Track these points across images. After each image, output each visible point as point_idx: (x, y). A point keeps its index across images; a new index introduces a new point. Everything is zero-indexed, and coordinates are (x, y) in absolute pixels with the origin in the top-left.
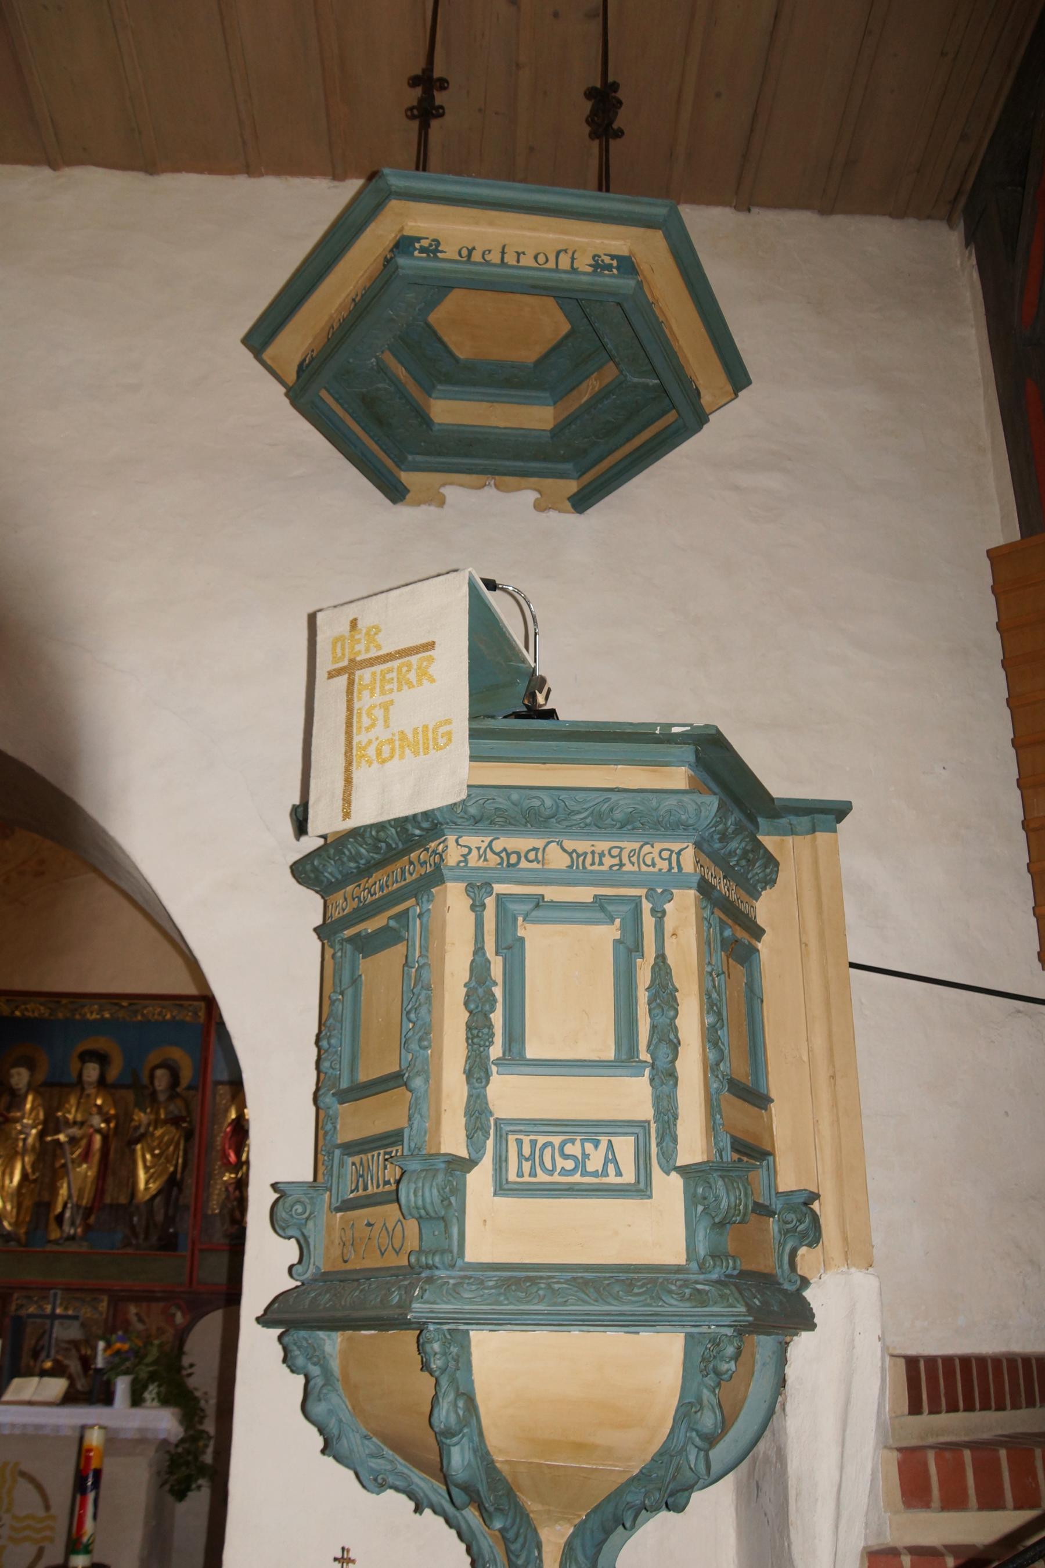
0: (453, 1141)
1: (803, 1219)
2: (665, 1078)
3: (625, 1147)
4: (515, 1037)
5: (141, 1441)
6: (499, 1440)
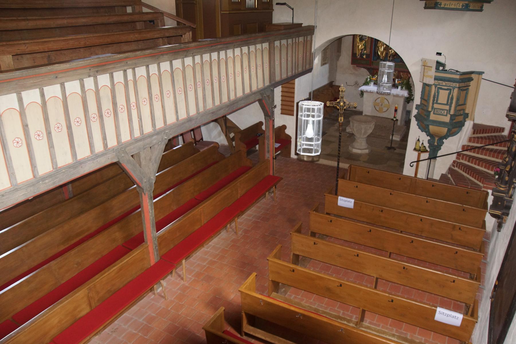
0: (430, 109)
2: (450, 107)
3: (446, 112)
4: (437, 100)
5: (402, 96)
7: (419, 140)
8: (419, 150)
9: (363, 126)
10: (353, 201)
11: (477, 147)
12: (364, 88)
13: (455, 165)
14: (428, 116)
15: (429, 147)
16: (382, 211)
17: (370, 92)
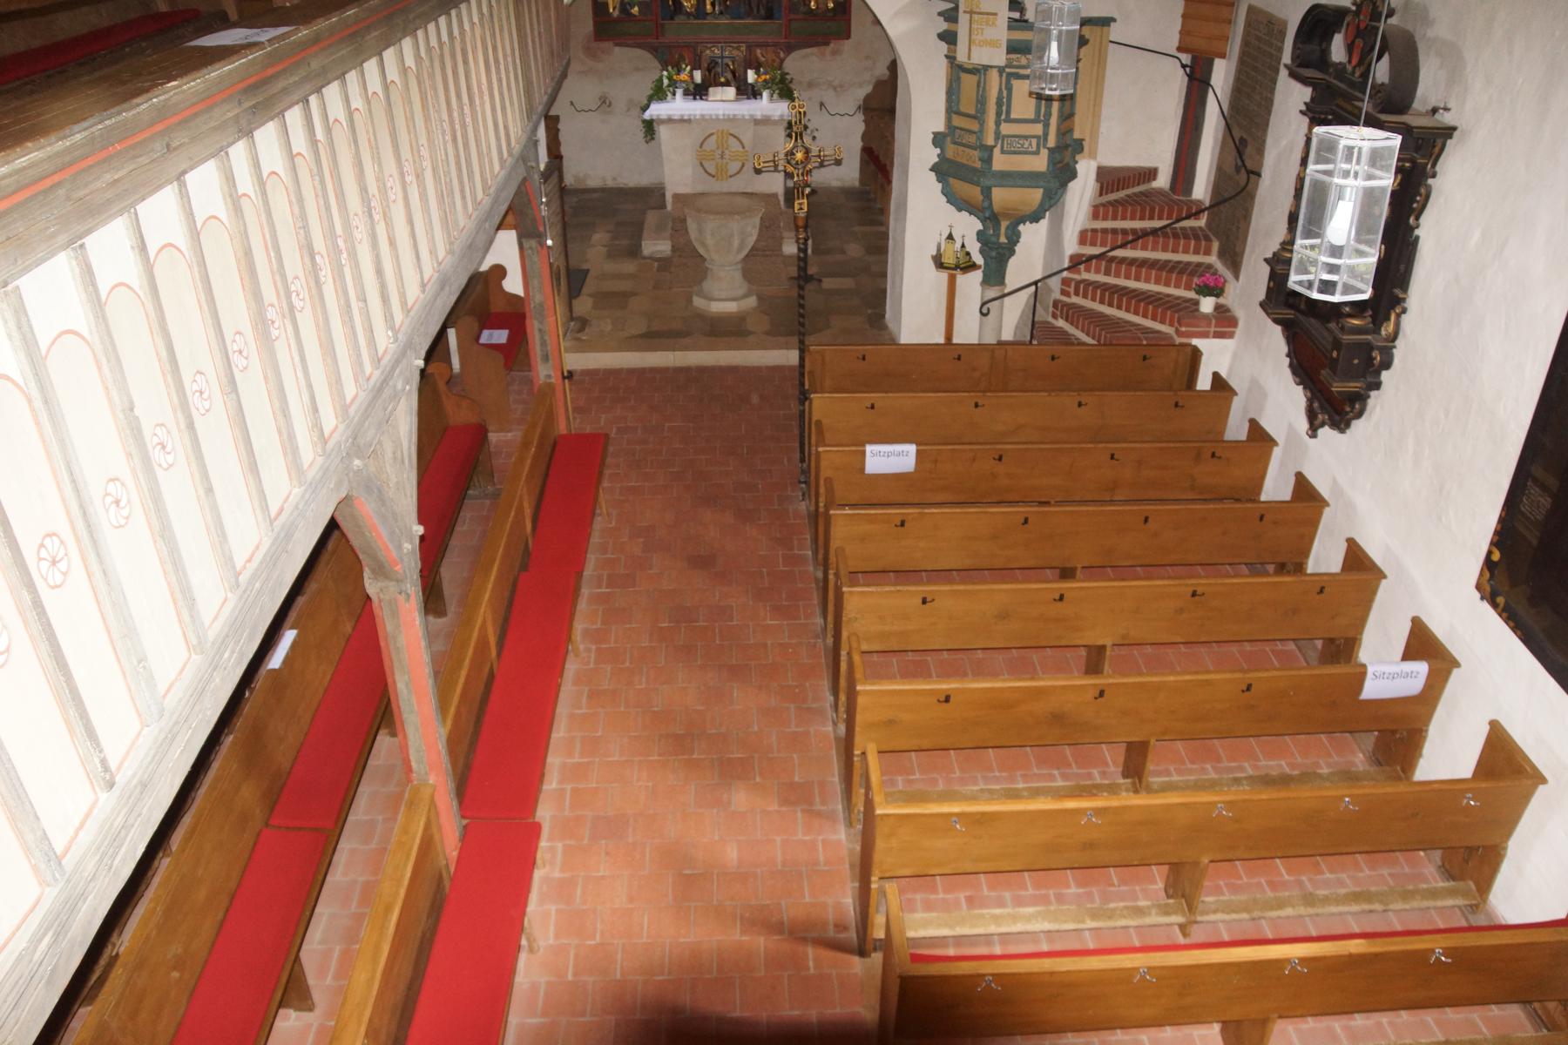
0: (990, 141)
1: (1078, 146)
2: (1047, 126)
3: (1034, 142)
4: (1008, 113)
6: (996, 207)
7: (950, 237)
8: (957, 267)
9: (735, 225)
10: (911, 449)
11: (1154, 232)
12: (657, 110)
13: (1072, 290)
14: (988, 161)
15: (981, 252)
16: (1000, 459)
17: (682, 121)
